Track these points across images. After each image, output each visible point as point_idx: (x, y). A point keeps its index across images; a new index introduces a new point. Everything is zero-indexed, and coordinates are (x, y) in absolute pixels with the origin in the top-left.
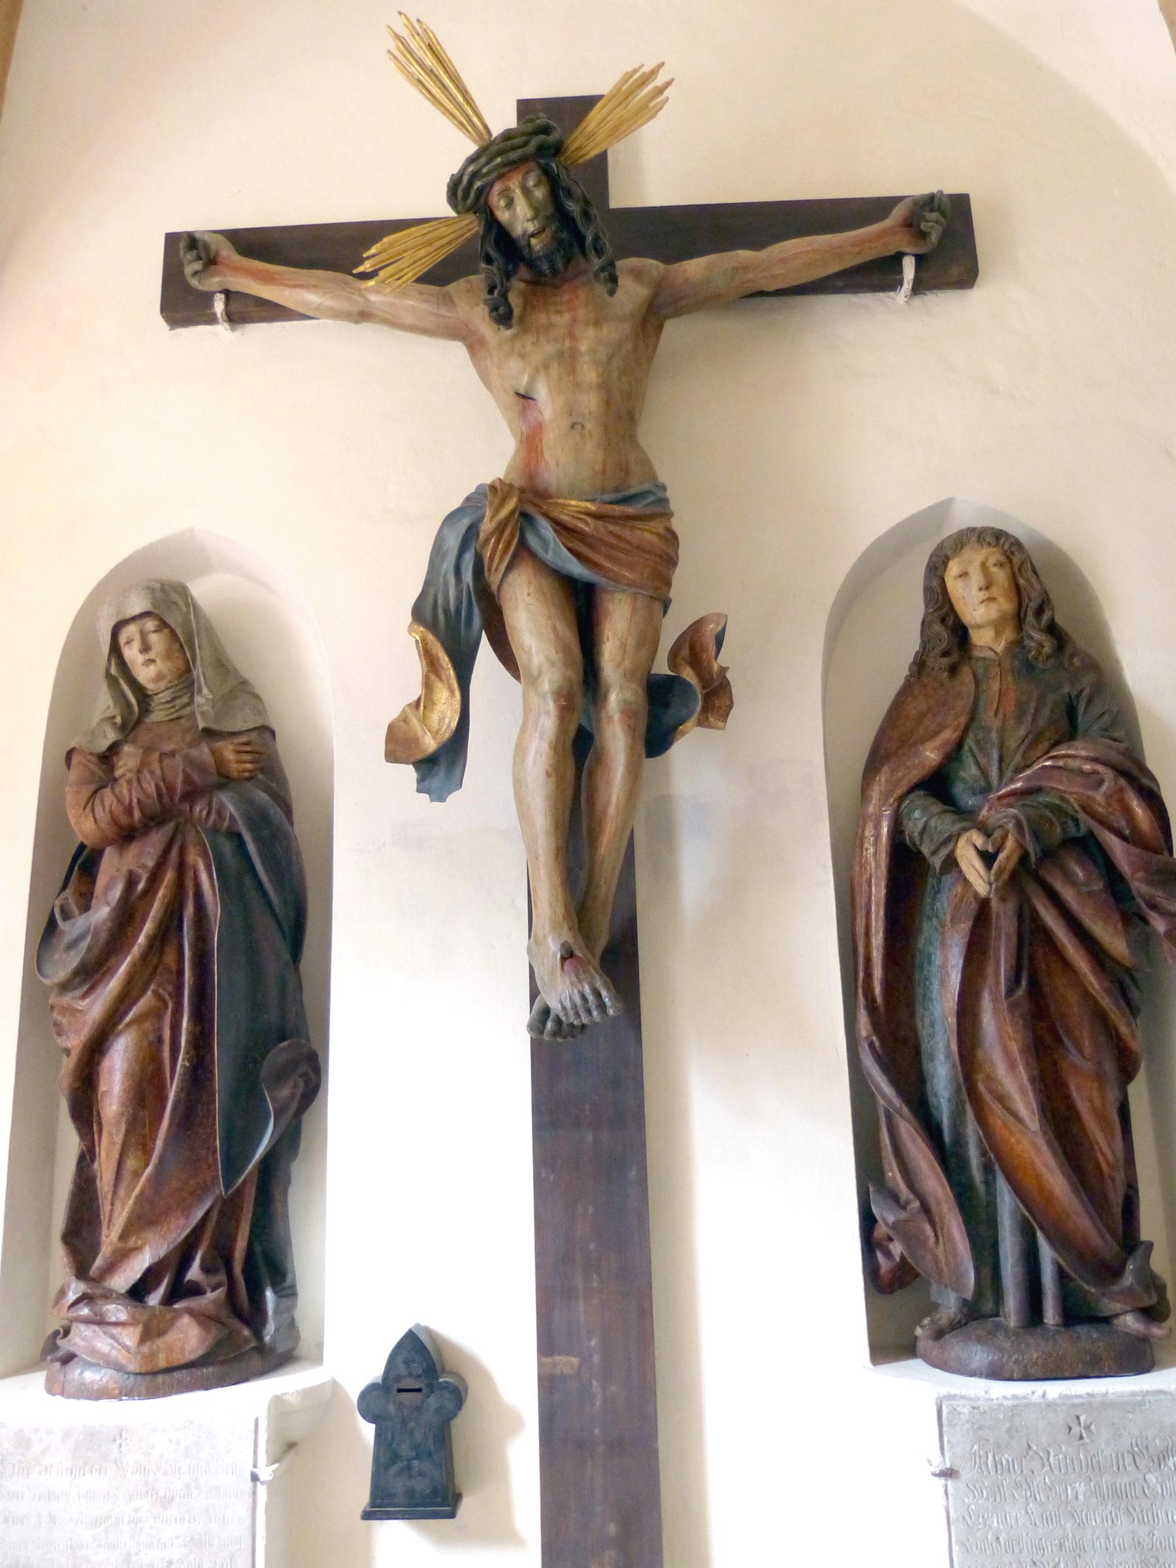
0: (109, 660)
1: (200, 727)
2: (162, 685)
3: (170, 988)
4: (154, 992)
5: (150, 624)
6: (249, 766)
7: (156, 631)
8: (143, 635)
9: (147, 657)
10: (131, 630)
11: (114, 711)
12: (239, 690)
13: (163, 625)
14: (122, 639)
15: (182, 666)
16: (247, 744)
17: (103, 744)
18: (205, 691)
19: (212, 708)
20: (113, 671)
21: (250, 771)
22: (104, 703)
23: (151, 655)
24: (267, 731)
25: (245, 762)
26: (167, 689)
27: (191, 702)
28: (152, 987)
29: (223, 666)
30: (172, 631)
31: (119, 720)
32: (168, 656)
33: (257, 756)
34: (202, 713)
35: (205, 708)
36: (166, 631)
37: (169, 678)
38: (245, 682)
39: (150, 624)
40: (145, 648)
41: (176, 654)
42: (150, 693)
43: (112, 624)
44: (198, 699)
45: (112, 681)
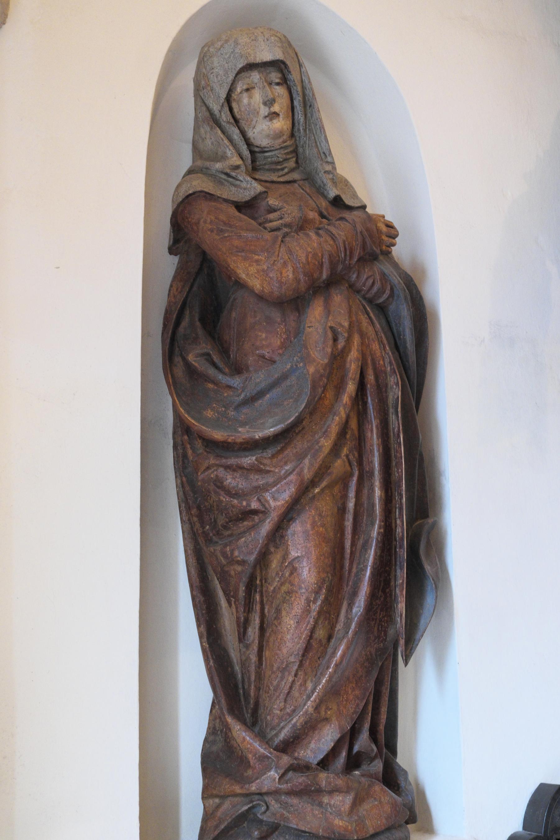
3: (356, 454)
4: (347, 456)
7: (278, 84)
10: (255, 76)
28: (345, 451)
37: (285, 137)
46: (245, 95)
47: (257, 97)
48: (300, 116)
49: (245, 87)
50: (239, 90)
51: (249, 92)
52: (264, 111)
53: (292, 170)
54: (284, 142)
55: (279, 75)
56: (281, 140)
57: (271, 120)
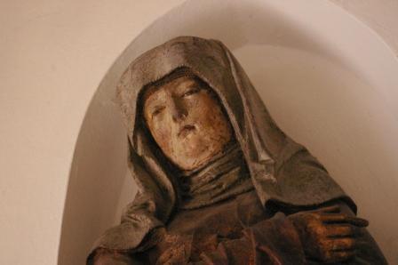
0: (135, 137)
1: (263, 201)
2: (204, 158)
5: (184, 86)
6: (347, 241)
7: (191, 92)
8: (178, 101)
9: (183, 124)
10: (162, 96)
11: (146, 198)
12: (300, 161)
13: (200, 85)
14: (149, 112)
15: (227, 135)
16: (337, 211)
17: (136, 238)
18: (263, 156)
19: (275, 176)
20: (140, 151)
21: (346, 250)
22: (131, 188)
23: (189, 121)
24: (347, 202)
25: (339, 237)
26: (210, 163)
27: (245, 173)
29: (277, 135)
30: (211, 91)
31: (152, 205)
32: (209, 122)
33: (355, 228)
34: (262, 182)
35: (266, 176)
36: (204, 91)
37: (212, 149)
38: (304, 151)
39: (184, 86)
40: (181, 111)
41: (218, 118)
42: (188, 174)
43: (137, 92)
44: (252, 166)
45: (137, 162)
46: (156, 118)
47: (168, 115)
48: (233, 119)
49: (153, 110)
50: (150, 116)
51: (159, 115)
52: (175, 128)
53: (234, 184)
54: (213, 155)
55: (191, 83)
56: (207, 154)
57: (185, 136)
